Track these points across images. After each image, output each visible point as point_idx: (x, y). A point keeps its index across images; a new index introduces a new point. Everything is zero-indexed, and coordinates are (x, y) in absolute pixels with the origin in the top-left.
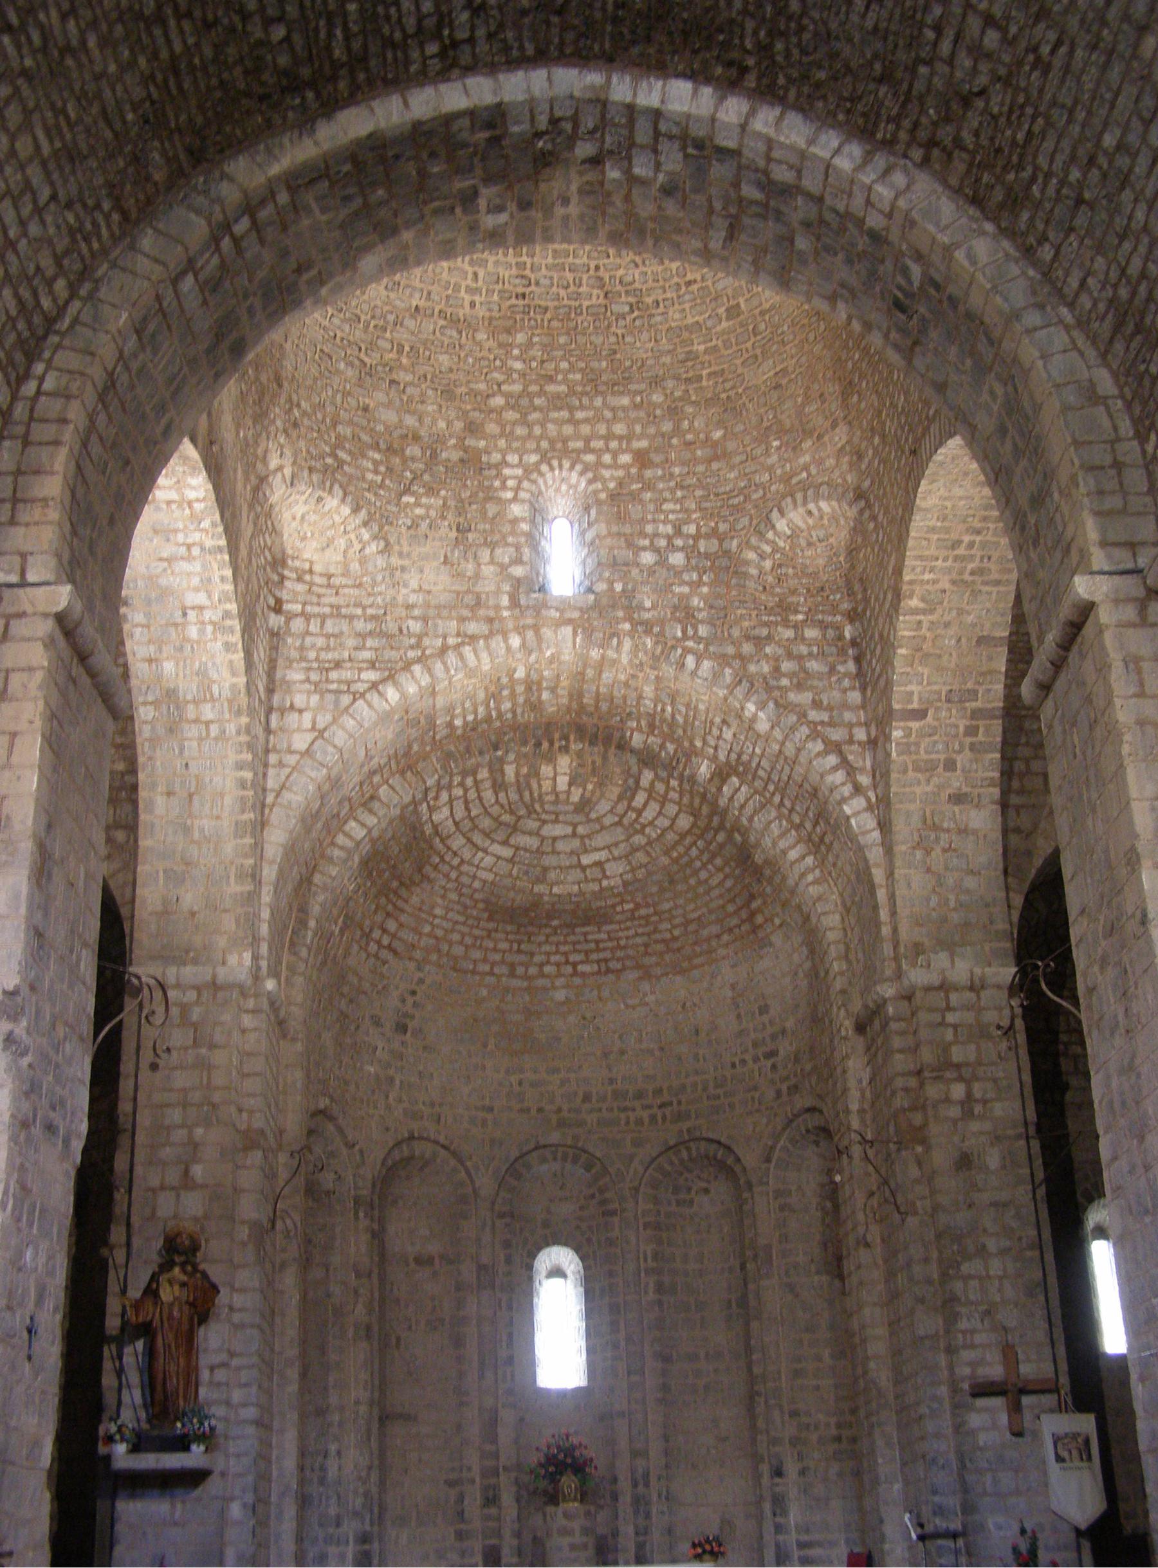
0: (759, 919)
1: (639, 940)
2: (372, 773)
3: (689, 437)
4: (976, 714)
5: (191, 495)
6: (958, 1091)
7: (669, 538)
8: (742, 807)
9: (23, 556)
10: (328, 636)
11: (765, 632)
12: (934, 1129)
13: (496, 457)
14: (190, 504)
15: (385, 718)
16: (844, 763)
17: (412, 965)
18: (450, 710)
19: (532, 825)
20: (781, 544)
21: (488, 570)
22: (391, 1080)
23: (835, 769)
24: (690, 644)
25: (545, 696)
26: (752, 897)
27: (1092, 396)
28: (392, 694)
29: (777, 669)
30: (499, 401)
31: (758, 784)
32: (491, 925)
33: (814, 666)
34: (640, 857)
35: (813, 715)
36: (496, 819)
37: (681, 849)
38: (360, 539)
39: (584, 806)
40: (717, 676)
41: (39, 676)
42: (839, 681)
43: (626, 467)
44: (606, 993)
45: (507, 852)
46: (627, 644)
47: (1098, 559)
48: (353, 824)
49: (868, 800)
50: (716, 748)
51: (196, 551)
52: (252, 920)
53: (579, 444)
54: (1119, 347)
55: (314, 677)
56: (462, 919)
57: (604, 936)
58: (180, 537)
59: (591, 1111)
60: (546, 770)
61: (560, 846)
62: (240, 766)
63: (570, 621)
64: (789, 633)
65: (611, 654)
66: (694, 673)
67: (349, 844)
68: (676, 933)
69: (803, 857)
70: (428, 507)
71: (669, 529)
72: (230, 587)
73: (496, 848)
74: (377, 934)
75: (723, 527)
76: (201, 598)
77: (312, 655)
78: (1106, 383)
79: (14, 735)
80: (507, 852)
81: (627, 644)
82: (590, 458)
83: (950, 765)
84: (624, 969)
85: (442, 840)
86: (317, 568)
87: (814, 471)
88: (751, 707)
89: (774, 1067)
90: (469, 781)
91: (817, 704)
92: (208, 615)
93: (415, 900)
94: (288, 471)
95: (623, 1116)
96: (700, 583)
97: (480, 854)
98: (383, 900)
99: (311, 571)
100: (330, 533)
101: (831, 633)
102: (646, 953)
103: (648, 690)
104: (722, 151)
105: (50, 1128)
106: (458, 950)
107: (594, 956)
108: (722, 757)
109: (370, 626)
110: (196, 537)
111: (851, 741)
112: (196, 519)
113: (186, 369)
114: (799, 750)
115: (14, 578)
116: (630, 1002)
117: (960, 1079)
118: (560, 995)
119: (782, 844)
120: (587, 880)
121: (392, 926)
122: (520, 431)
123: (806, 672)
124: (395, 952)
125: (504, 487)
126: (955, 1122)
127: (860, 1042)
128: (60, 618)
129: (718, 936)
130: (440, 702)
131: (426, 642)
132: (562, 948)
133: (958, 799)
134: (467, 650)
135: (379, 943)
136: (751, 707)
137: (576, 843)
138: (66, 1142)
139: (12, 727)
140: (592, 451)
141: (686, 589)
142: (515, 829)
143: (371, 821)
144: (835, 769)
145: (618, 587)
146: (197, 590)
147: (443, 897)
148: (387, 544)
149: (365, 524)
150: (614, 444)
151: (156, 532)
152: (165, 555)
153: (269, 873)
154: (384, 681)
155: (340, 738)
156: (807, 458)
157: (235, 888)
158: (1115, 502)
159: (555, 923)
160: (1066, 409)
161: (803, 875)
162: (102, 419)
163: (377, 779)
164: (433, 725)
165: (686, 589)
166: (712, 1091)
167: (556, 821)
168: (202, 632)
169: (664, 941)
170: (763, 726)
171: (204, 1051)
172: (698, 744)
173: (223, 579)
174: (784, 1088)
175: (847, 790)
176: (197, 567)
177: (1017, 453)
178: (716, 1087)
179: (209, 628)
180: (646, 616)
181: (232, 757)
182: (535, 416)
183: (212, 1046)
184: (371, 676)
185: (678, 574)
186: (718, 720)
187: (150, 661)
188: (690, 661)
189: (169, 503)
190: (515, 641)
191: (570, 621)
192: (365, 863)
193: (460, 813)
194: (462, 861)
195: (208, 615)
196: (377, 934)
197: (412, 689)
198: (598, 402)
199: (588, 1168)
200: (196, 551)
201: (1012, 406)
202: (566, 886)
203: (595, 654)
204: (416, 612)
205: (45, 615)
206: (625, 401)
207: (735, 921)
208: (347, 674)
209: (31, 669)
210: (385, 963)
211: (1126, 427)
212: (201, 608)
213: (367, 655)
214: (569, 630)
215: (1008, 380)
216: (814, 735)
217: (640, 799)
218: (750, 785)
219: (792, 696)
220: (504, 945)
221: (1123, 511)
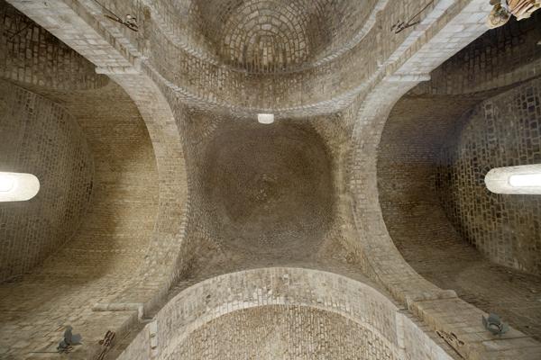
34: (239, 18)
45: (282, 18)
76: (358, 151)
92: (357, 146)
137: (260, 21)
142: (279, 28)
194: (297, 18)
195: (357, 146)
212: (359, 148)
217: (241, 49)
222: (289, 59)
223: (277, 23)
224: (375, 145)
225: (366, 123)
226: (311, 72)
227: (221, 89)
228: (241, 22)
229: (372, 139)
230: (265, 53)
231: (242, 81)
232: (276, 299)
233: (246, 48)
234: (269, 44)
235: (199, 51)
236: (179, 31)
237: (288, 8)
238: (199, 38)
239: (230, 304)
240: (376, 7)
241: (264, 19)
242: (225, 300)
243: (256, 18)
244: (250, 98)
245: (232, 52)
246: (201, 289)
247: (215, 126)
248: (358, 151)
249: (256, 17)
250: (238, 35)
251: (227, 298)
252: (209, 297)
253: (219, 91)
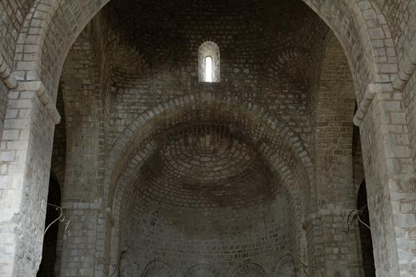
2: (145, 140)
3: (252, 30)
4: (344, 124)
5: (85, 48)
6: (336, 250)
7: (244, 64)
8: (267, 153)
9: (26, 71)
10: (131, 94)
11: (274, 96)
12: (328, 263)
13: (188, 36)
14: (85, 51)
15: (149, 121)
16: (300, 139)
17: (157, 203)
18: (170, 119)
19: (198, 157)
20: (281, 66)
21: (184, 74)
22: (149, 241)
23: (297, 141)
24: (250, 99)
25: (202, 115)
27: (378, 24)
28: (151, 114)
29: (278, 108)
30: (189, 17)
31: (272, 145)
32: (184, 190)
33: (291, 107)
34: (234, 169)
35: (291, 124)
36: (185, 155)
38: (141, 62)
39: (215, 151)
40: (259, 110)
41: (29, 111)
42: (299, 112)
43: (230, 40)
45: (189, 166)
46: (229, 99)
47: (377, 78)
48: (138, 156)
49: (308, 152)
50: (258, 133)
51: (87, 66)
52: (101, 188)
53: (215, 32)
54: (387, 8)
55: (125, 108)
56: (174, 188)
58: (82, 62)
59: (215, 253)
60: (202, 139)
61: (207, 165)
62: (100, 137)
63: (210, 91)
64: (283, 96)
65: (224, 102)
66: (251, 109)
67: (136, 163)
69: (287, 170)
70: (165, 52)
71: (244, 61)
73: (186, 165)
74: (145, 192)
75: (261, 61)
76: (88, 82)
77: (125, 101)
78: (382, 20)
79: (21, 130)
80: (189, 166)
81: (229, 99)
82: (219, 37)
83: (335, 141)
85: (168, 162)
86: (127, 72)
87: (292, 42)
88: (270, 120)
89: (276, 240)
90: (177, 143)
91: (292, 120)
92: (91, 87)
93: (158, 181)
94: (118, 40)
95: (226, 255)
96: (253, 79)
98: (148, 181)
99: (125, 73)
100: (132, 60)
101: (297, 96)
103: (236, 114)
105: (29, 259)
106: (173, 198)
108: (260, 136)
109: (145, 91)
110: (87, 62)
111: (303, 132)
112: (87, 56)
113: (81, 10)
114: (285, 135)
115: (23, 79)
117: (337, 246)
118: (206, 214)
119: (280, 166)
120: (215, 176)
121: (150, 190)
122: (196, 28)
123: (288, 109)
124: (152, 199)
125: (190, 46)
126: (335, 261)
127: (304, 232)
128: (37, 92)
130: (167, 117)
131: (163, 97)
133: (338, 152)
134: (176, 100)
135: (146, 195)
136: (270, 120)
137: (212, 163)
138: (34, 263)
139: (21, 128)
140: (219, 35)
141: (249, 81)
142: (192, 159)
143: (144, 155)
144: (297, 141)
145: (227, 80)
146: (87, 79)
147: (168, 181)
148: (151, 64)
149: (144, 58)
150: (226, 33)
152: (76, 67)
153: (109, 172)
154: (148, 110)
155: (134, 128)
156: (290, 38)
157: (97, 177)
158: (384, 59)
160: (368, 28)
161: (286, 176)
162: (53, 26)
163: (146, 141)
164: (165, 124)
165: (249, 81)
166: (255, 247)
167: (205, 156)
168: (89, 93)
170: (273, 127)
171: (85, 231)
172: (253, 132)
174: (279, 247)
175: (301, 149)
176: (87, 72)
177: (353, 42)
178: (257, 246)
179: (91, 92)
180: (236, 90)
181: (97, 134)
182: (201, 22)
183: (88, 230)
184: (144, 108)
185: (246, 76)
186: (259, 125)
187: (71, 102)
188: (250, 105)
189: (78, 51)
190: (192, 98)
191: (210, 91)
192: (141, 169)
193: (174, 153)
195: (91, 87)
196: (145, 192)
197: (158, 112)
198: (222, 18)
199: (214, 272)
201: (352, 26)
202: (209, 178)
203: (218, 102)
204: (160, 87)
205: (32, 91)
206: (231, 18)
208: (136, 107)
209: (26, 109)
210: (148, 202)
211: (388, 35)
212: (88, 85)
213: (143, 101)
214: (210, 94)
215: (350, 18)
216: (290, 130)
217: (233, 149)
218: (270, 145)
219: (283, 117)
220: (187, 197)
221: (386, 63)
223: (194, 162)
225: (90, 119)
226: (156, 136)
228: (231, 166)
233: (229, 148)
234: (203, 149)
235: (278, 164)
237: (183, 174)
240: (118, 230)
241: (207, 165)
243: (216, 166)
245: (245, 149)
247: (281, 60)
248: (88, 82)
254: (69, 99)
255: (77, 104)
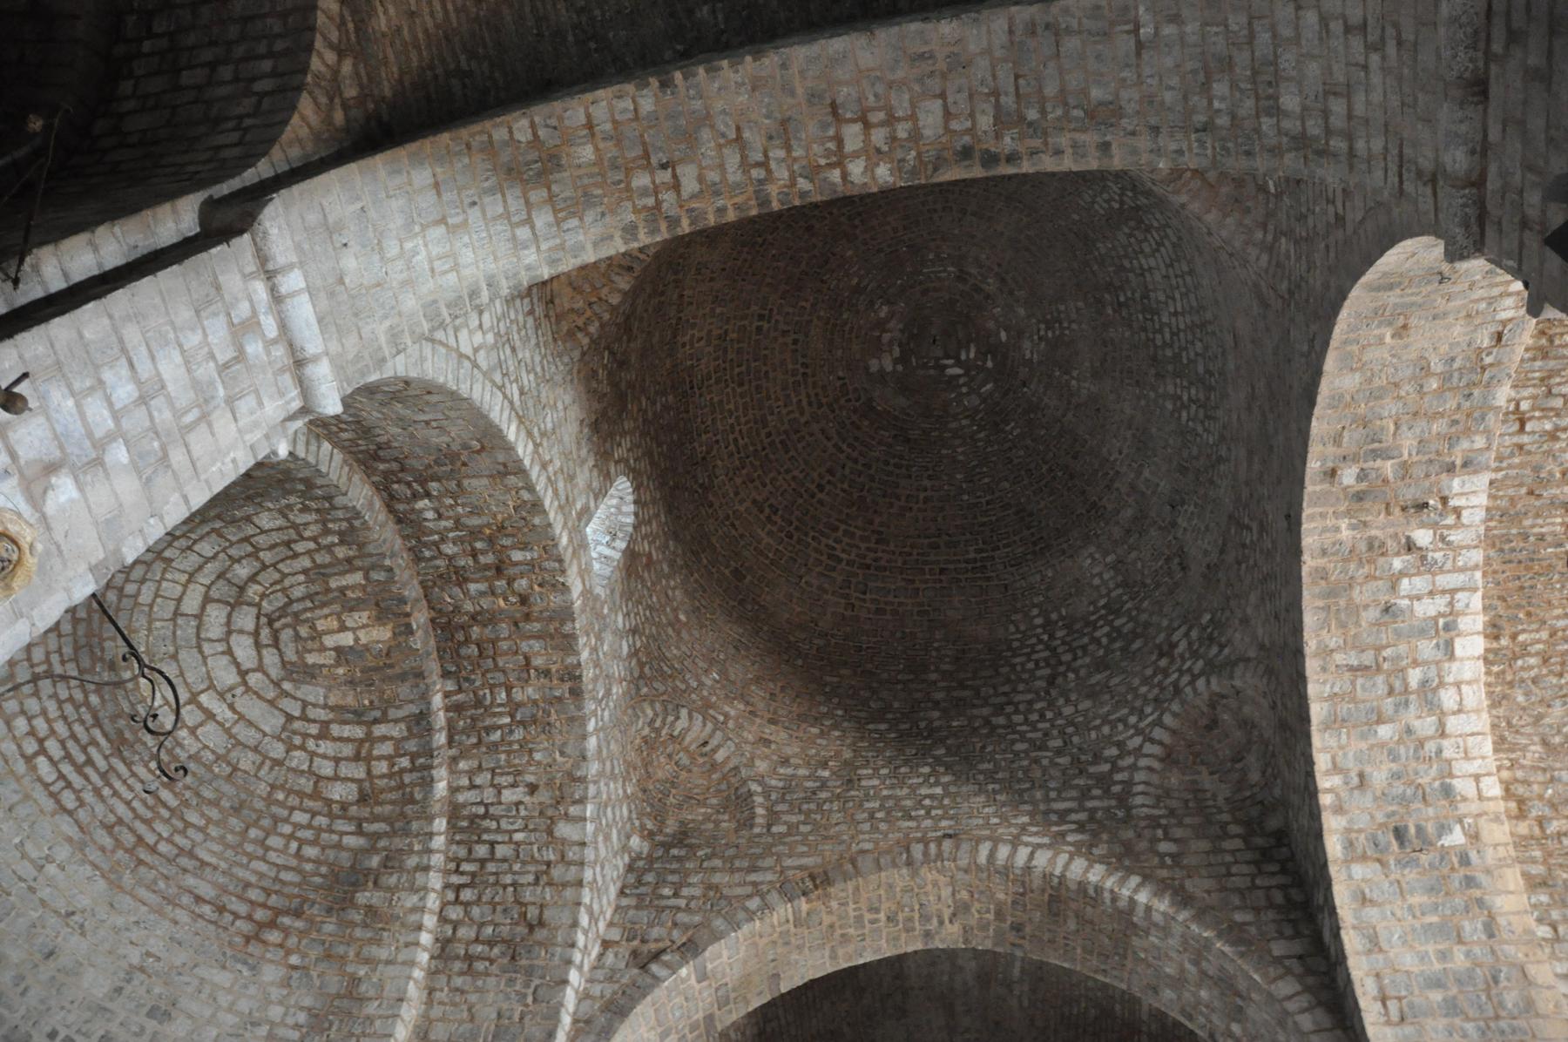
0: (274, 936)
1: (121, 809)
5: (856, 169)
14: (839, 164)
20: (664, 732)
26: (298, 914)
34: (247, 761)
37: (293, 801)
38: (588, 321)
44: (22, 811)
45: (191, 604)
51: (757, 173)
57: (102, 764)
68: (163, 847)
72: (712, 220)
76: (690, 185)
84: (70, 813)
92: (668, 197)
97: (184, 578)
102: (109, 828)
104: (1449, 645)
107: (66, 769)
110: (782, 174)
116: (29, 847)
129: (199, 899)
132: (78, 728)
137: (231, 678)
146: (701, 179)
151: (784, 122)
152: (746, 134)
159: (94, 699)
168: (644, 192)
169: (140, 839)
173: (721, 211)
176: (734, 175)
179: (651, 201)
187: (590, 126)
195: (668, 197)
200: (757, 173)
207: (242, 909)
212: (676, 186)
222: (341, 552)
223: (216, 615)
224: (647, 104)
225: (543, 219)
227: (533, 789)
229: (617, 138)
230: (347, 639)
231: (479, 703)
232: (1457, 511)
234: (304, 631)
236: (371, 1008)
237: (145, 597)
238: (371, 910)
239: (1452, 723)
242: (1430, 747)
244: (538, 662)
245: (382, 767)
246: (1358, 870)
247: (682, 723)
249: (221, 695)
250: (313, 754)
251: (1421, 744)
252: (1399, 834)
253: (544, 796)
254: (600, 112)
255: (587, 153)
